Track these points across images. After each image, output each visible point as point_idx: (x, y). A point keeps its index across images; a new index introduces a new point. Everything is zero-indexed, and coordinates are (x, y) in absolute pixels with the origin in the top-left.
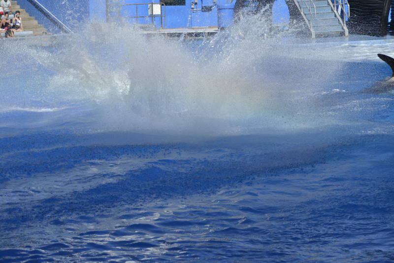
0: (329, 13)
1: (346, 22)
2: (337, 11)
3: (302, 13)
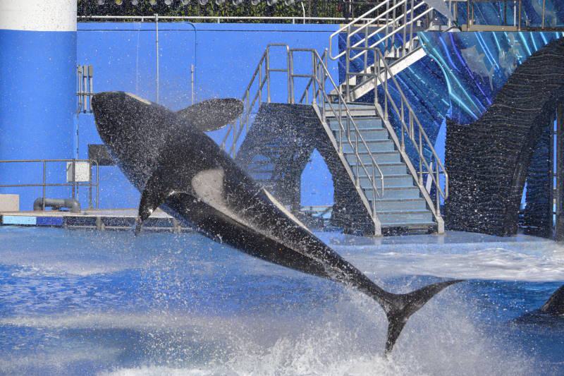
0: (410, 188)
1: (441, 206)
2: (425, 185)
3: (358, 188)
